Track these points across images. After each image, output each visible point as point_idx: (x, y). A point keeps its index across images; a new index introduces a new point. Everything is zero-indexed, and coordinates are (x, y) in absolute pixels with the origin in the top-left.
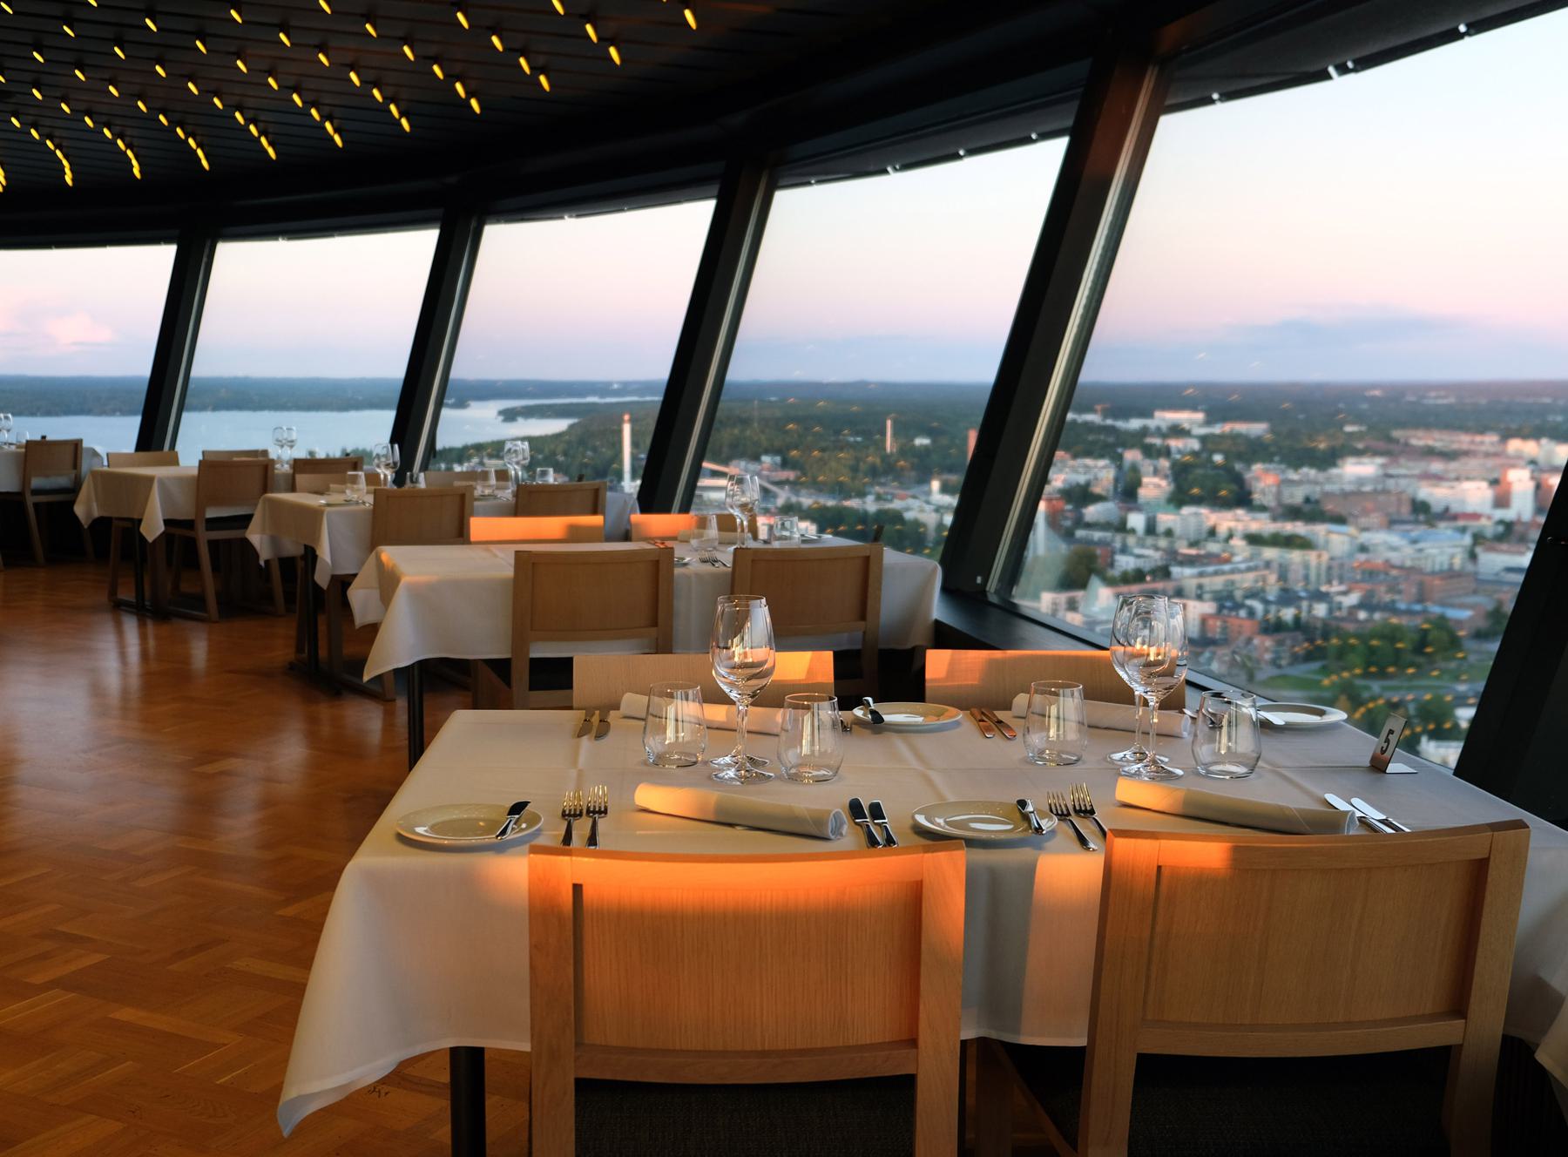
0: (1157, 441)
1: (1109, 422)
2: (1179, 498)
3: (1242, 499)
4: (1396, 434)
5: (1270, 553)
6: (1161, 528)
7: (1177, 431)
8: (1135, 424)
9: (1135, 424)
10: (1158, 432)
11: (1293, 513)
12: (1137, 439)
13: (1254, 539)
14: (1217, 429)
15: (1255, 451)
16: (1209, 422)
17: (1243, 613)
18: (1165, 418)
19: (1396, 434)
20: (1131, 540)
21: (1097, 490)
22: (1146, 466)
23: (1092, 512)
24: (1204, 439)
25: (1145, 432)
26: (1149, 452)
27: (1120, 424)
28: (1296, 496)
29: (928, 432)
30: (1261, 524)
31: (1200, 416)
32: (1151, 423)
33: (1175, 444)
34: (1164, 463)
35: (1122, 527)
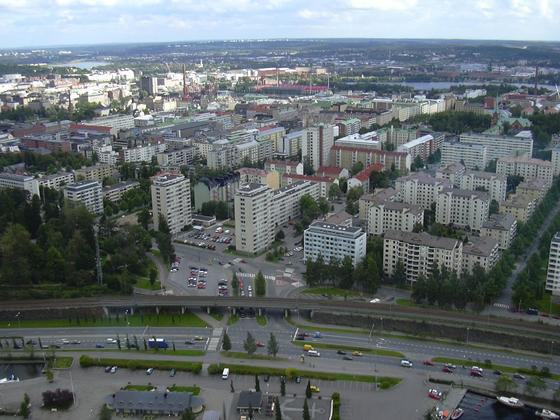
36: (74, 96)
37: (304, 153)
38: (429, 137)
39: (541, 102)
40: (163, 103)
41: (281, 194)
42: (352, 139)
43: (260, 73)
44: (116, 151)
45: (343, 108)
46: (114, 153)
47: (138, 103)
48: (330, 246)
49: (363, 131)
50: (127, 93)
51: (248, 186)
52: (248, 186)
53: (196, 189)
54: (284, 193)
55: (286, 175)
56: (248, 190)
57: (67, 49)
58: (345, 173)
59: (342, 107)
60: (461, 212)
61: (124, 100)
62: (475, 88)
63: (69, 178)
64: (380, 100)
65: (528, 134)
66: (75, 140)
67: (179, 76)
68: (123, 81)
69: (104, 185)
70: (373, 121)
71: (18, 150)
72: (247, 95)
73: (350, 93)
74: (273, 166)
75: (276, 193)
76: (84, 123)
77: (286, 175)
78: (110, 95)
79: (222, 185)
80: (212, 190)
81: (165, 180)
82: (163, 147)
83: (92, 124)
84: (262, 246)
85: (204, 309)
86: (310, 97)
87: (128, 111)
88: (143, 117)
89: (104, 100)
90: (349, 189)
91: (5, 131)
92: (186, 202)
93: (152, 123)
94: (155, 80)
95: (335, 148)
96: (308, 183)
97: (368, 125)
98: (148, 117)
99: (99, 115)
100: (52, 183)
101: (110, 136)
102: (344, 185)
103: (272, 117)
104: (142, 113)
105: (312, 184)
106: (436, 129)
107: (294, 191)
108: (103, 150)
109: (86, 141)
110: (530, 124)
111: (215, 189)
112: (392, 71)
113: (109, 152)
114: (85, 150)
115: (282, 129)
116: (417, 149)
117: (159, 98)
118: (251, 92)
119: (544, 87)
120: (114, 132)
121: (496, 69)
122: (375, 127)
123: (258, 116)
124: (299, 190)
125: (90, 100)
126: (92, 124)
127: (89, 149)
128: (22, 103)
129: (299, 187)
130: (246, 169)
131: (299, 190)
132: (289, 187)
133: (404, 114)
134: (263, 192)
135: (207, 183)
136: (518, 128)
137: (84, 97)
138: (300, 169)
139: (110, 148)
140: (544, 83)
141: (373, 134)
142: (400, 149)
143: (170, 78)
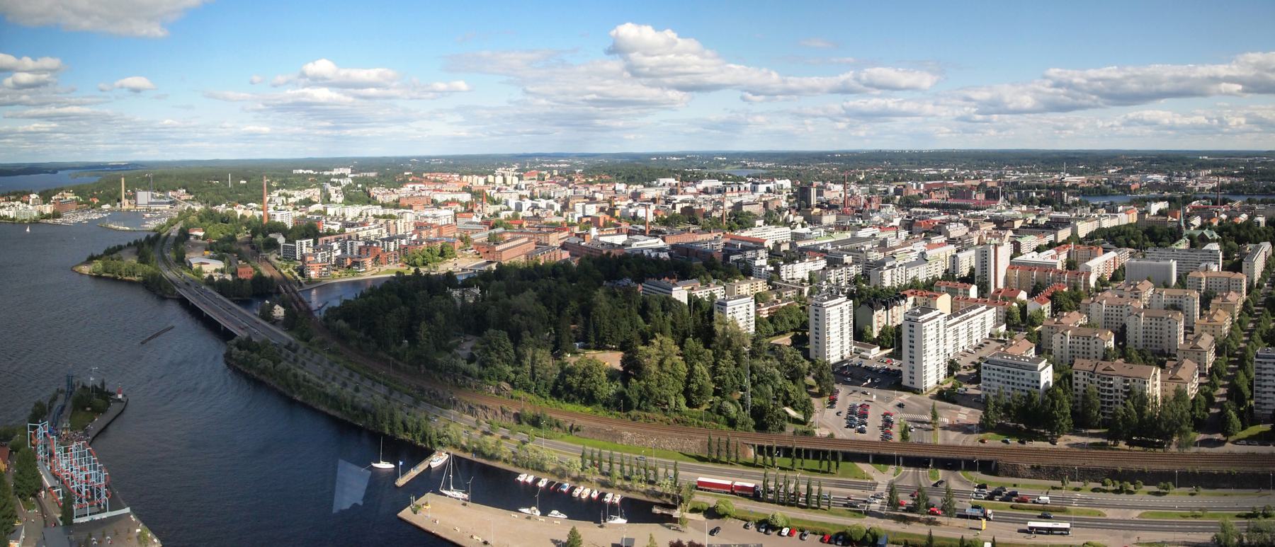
0: (336, 180)
3: (370, 200)
5: (382, 221)
12: (328, 179)
15: (369, 182)
20: (328, 219)
23: (313, 208)
24: (352, 179)
26: (333, 184)
30: (380, 211)
33: (341, 181)
34: (339, 188)
35: (324, 213)
36: (728, 204)
37: (977, 273)
38: (1112, 254)
39: (1225, 213)
40: (821, 215)
42: (1029, 256)
43: (926, 186)
45: (1018, 224)
47: (794, 216)
48: (1011, 380)
49: (1039, 250)
50: (784, 204)
51: (918, 311)
57: (723, 155)
58: (1023, 295)
59: (1016, 222)
60: (1154, 335)
61: (780, 210)
62: (1156, 200)
64: (1057, 214)
65: (1215, 247)
66: (728, 251)
67: (839, 187)
68: (779, 190)
69: (756, 301)
70: (1051, 237)
71: (668, 256)
72: (913, 210)
73: (1024, 208)
75: (949, 318)
78: (766, 204)
79: (887, 309)
80: (876, 313)
81: (825, 301)
83: (746, 234)
85: (864, 458)
86: (981, 212)
87: (786, 223)
88: (799, 229)
89: (757, 209)
90: (1028, 314)
91: (657, 237)
94: (813, 191)
95: (1013, 266)
96: (984, 308)
97: (1046, 241)
98: (806, 230)
99: (753, 226)
100: (702, 293)
101: (764, 248)
102: (1023, 308)
103: (940, 234)
104: (799, 226)
105: (988, 308)
106: (1119, 246)
107: (968, 318)
108: (758, 263)
109: (738, 252)
110: (1216, 236)
111: (880, 312)
112: (1067, 185)
114: (737, 261)
115: (952, 247)
116: (1101, 267)
117: (817, 210)
118: (917, 207)
119: (1226, 197)
120: (769, 244)
121: (1176, 180)
122: (1051, 245)
124: (974, 315)
125: (745, 209)
126: (746, 234)
128: (674, 207)
129: (974, 312)
130: (912, 290)
131: (974, 315)
132: (963, 312)
133: (1084, 229)
134: (935, 317)
135: (871, 306)
136: (1205, 240)
137: (738, 206)
138: (973, 291)
139: (764, 262)
140: (1225, 194)
141: (1053, 252)
142: (1081, 268)
143: (830, 189)
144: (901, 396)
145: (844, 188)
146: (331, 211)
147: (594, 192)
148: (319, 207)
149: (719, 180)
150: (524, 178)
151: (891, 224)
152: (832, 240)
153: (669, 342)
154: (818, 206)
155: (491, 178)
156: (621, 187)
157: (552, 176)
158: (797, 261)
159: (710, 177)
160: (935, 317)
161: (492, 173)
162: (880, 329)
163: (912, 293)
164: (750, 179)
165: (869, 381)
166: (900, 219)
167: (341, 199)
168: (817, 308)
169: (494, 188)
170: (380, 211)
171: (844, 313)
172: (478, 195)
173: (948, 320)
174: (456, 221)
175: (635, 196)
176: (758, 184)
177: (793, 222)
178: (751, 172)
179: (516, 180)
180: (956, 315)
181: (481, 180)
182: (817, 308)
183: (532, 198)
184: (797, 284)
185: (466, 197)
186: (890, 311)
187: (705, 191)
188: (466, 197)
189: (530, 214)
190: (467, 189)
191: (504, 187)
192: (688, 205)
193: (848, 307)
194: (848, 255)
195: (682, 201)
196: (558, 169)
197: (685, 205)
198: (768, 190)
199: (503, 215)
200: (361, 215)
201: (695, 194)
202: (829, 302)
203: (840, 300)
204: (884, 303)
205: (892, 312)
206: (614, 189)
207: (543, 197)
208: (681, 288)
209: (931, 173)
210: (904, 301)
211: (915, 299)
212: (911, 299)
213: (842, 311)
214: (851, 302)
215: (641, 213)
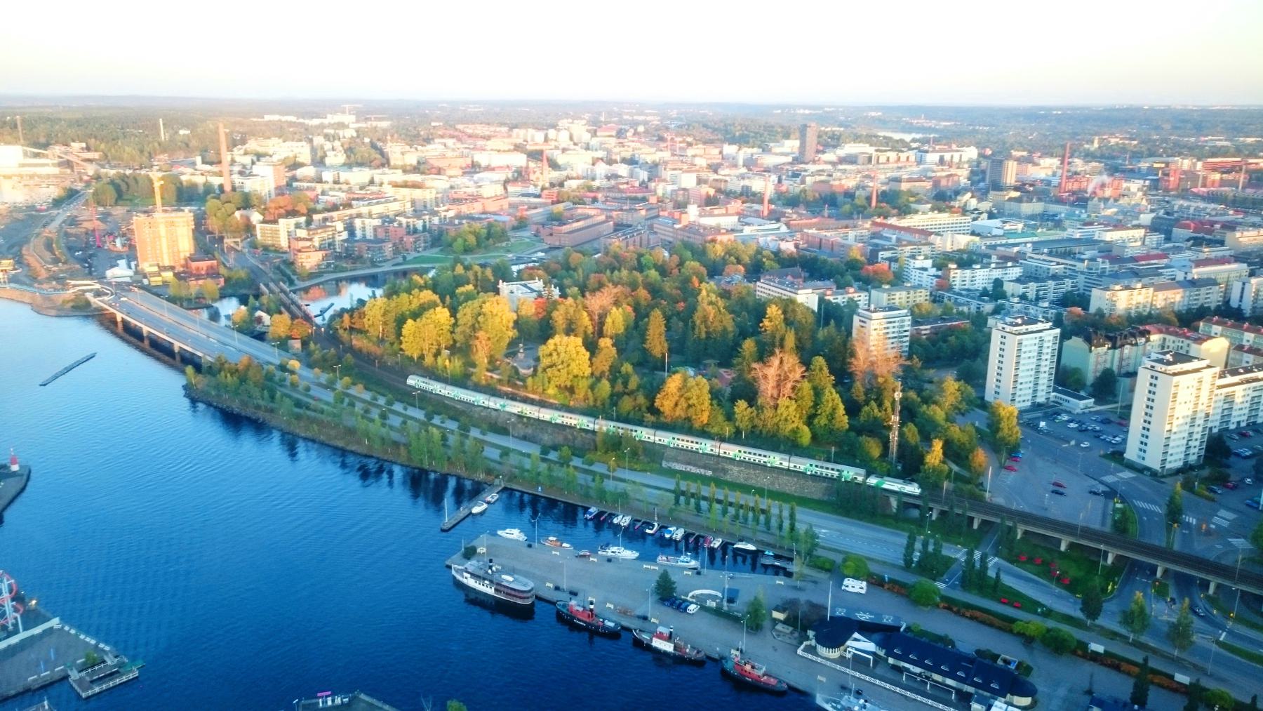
0: (332, 132)
1: (301, 120)
2: (349, 165)
3: (385, 163)
4: (460, 127)
6: (342, 180)
7: (342, 126)
8: (316, 122)
9: (316, 122)
10: (331, 126)
11: (416, 169)
13: (396, 185)
14: (363, 125)
16: (357, 121)
17: (396, 224)
18: (331, 119)
19: (460, 127)
21: (300, 160)
22: (328, 146)
23: (300, 172)
25: (322, 126)
27: (307, 122)
28: (412, 159)
29: (186, 126)
30: (399, 177)
31: (353, 118)
32: (326, 121)
33: (341, 133)
34: (337, 144)
35: (319, 180)
41: (1230, 379)
44: (939, 269)
46: (933, 271)
51: (1169, 357)
52: (1169, 357)
53: (1066, 343)
54: (1236, 379)
55: (1240, 348)
56: (1169, 363)
57: (877, 109)
63: (861, 298)
66: (877, 245)
74: (1217, 329)
75: (1222, 376)
76: (893, 221)
77: (1240, 348)
79: (1114, 347)
81: (1017, 325)
82: (1016, 272)
83: (906, 222)
84: (1175, 462)
91: (778, 220)
92: (1047, 366)
93: (1000, 232)
113: (925, 269)
114: (890, 260)
123: (1195, 239)
126: (906, 222)
127: (895, 260)
128: (803, 182)
134: (1197, 370)
135: (1088, 340)
139: (928, 263)
144: (1121, 471)
145: (1062, 163)
146: (328, 176)
147: (694, 156)
148: (309, 171)
149: (871, 145)
150: (598, 134)
151: (1135, 222)
152: (1035, 239)
153: (791, 360)
154: (1016, 189)
155: (552, 133)
156: (729, 149)
157: (636, 133)
158: (978, 266)
159: (857, 138)
160: (1197, 370)
161: (554, 126)
162: (1098, 374)
163: (1160, 332)
164: (914, 145)
165: (1073, 443)
166: (1153, 215)
167: (341, 158)
168: (1004, 334)
169: (557, 148)
170: (399, 177)
171: (1045, 345)
172: (536, 155)
173: (1220, 377)
174: (505, 189)
175: (750, 164)
176: (927, 152)
177: (976, 209)
178: (918, 136)
179: (586, 137)
180: (1234, 373)
181: (539, 137)
182: (1004, 334)
183: (610, 162)
184: (974, 298)
185: (520, 160)
186: (1117, 351)
187: (851, 160)
188: (520, 160)
189: (605, 183)
190: (518, 148)
191: (572, 147)
192: (823, 178)
193: (1051, 338)
194: (1058, 264)
195: (813, 175)
196: (645, 123)
197: (818, 178)
198: (942, 161)
199: (572, 184)
200: (372, 182)
201: (833, 164)
202: (1024, 328)
203: (1040, 326)
204: (1109, 338)
205: (1122, 353)
206: (721, 152)
207: (624, 161)
208: (810, 291)
209: (1219, 144)
210: (1143, 340)
211: (1165, 339)
212: (1155, 338)
213: (1042, 340)
214: (1058, 331)
215: (757, 185)
